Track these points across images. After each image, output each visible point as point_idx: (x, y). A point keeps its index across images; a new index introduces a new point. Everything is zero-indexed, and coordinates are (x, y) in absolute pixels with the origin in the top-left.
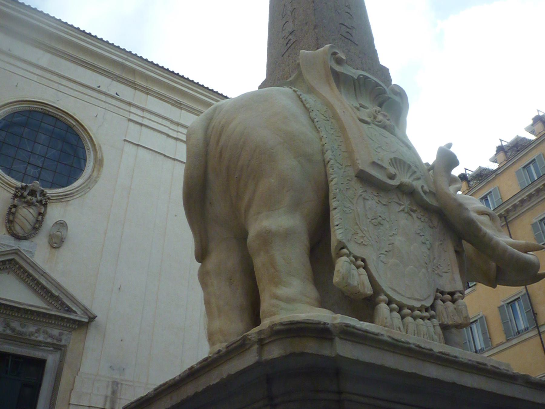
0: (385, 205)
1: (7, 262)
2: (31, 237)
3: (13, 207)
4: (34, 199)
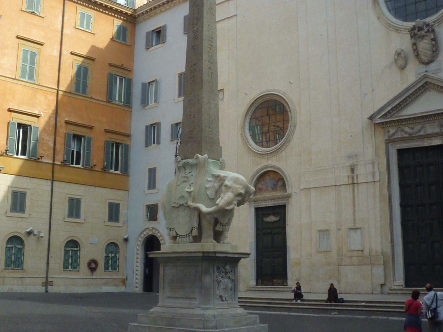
1: (425, 85)
2: (435, 59)
3: (414, 46)
4: (423, 32)
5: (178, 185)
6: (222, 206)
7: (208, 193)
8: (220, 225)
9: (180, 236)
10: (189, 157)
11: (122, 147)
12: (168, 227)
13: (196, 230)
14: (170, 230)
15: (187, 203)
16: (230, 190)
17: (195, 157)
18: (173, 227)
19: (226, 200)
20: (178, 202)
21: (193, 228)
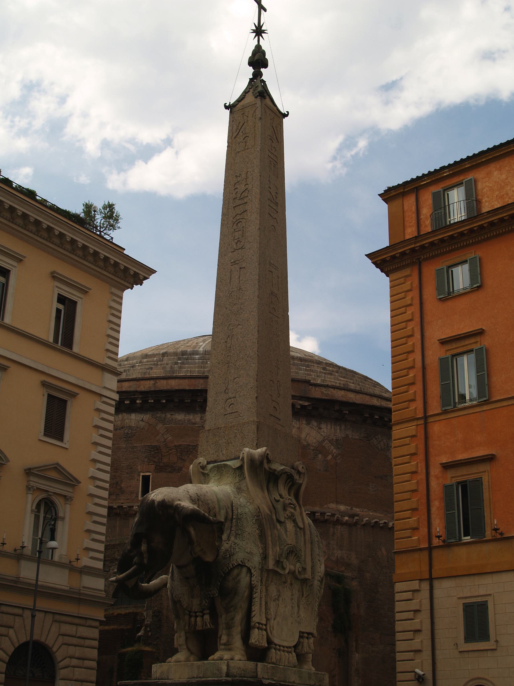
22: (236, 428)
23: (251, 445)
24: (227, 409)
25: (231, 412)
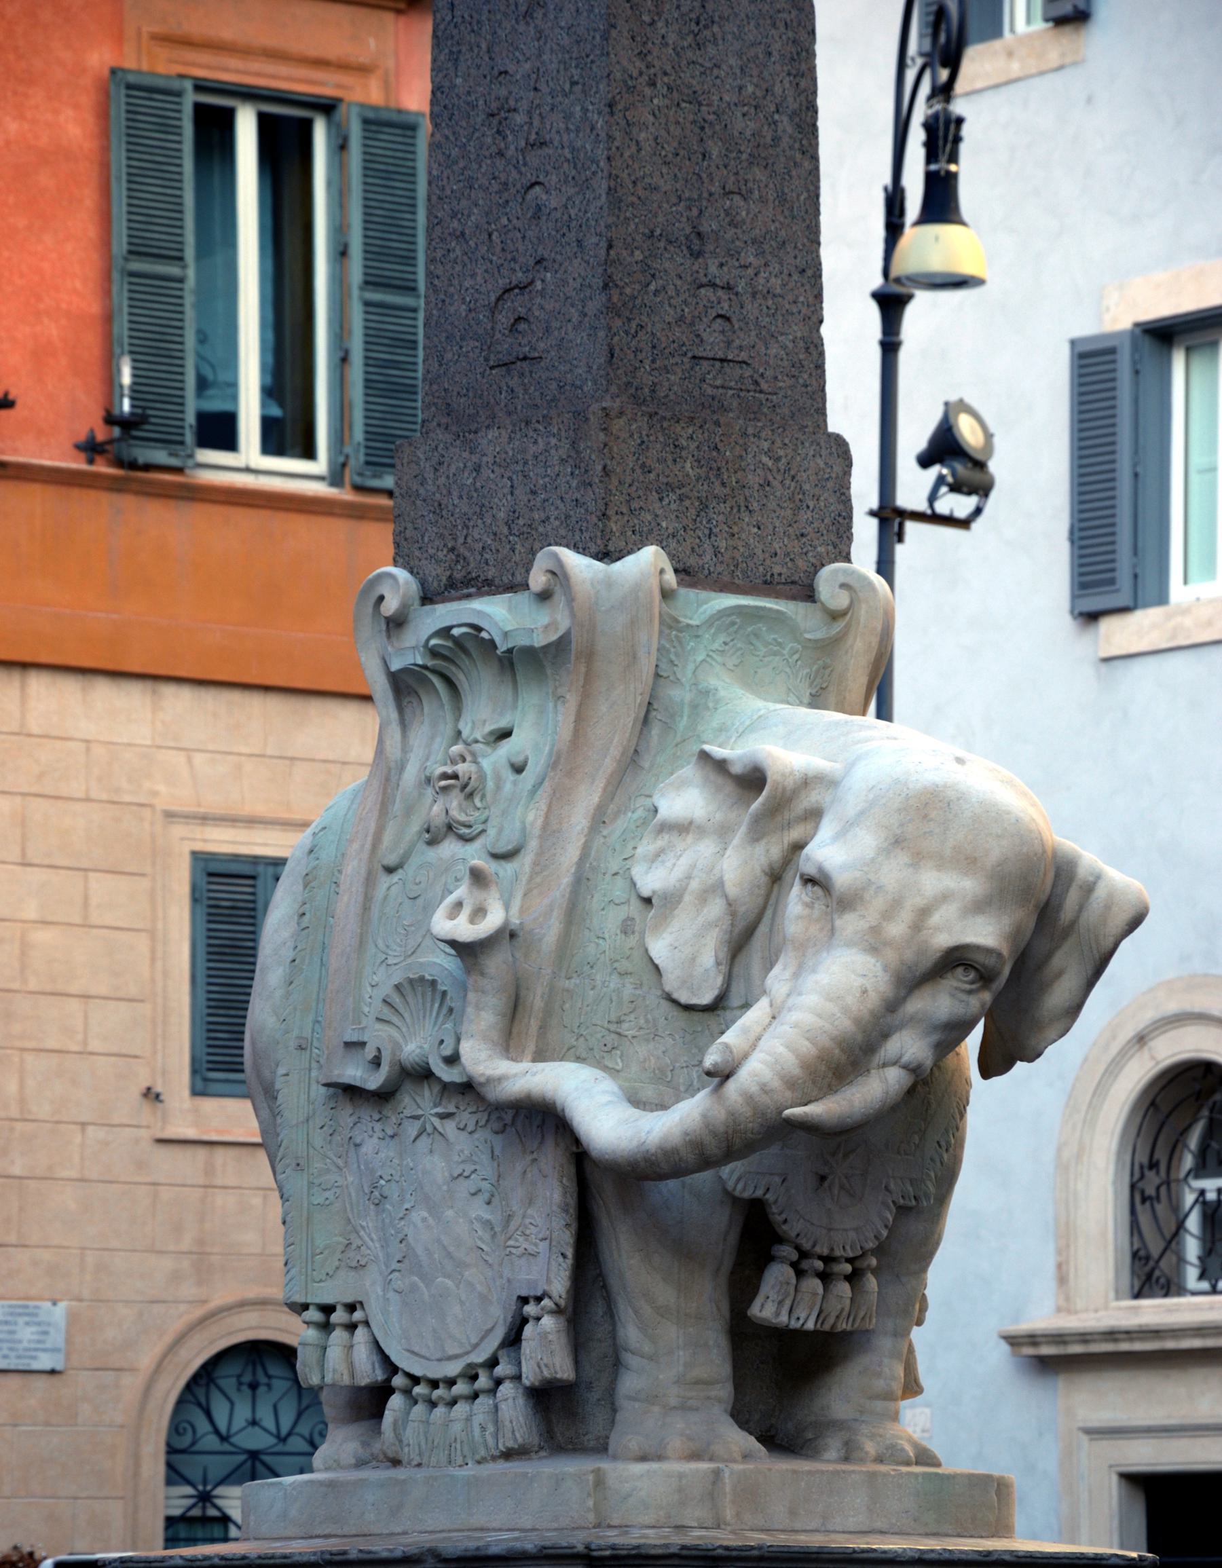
0: (392, 1137)
5: (390, 870)
6: (764, 1088)
7: (660, 948)
8: (800, 1273)
9: (418, 1390)
10: (491, 573)
11: (340, 146)
12: (300, 1298)
13: (548, 1322)
14: (326, 1327)
15: (453, 1060)
16: (850, 924)
17: (538, 579)
18: (349, 1300)
19: (796, 1026)
20: (377, 1036)
21: (530, 1309)
22: (766, 445)
23: (830, 548)
24: (704, 335)
25: (720, 355)
